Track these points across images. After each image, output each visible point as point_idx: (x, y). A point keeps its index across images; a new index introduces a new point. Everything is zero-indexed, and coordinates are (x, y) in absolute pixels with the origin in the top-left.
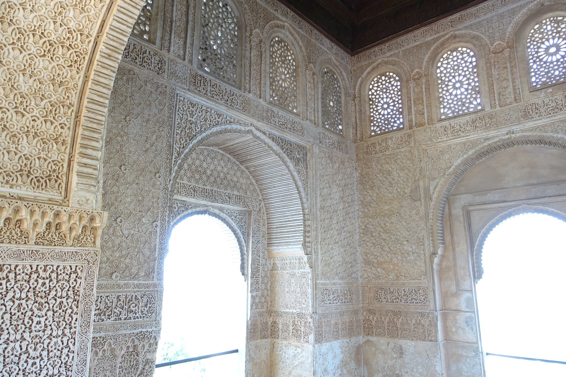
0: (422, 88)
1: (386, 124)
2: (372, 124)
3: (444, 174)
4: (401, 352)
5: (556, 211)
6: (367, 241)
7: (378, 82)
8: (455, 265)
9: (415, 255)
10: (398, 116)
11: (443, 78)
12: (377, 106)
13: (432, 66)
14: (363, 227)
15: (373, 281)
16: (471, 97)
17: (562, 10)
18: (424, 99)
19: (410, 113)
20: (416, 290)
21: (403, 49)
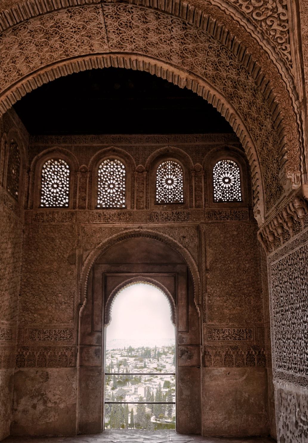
0: (86, 180)
1: (54, 200)
2: (42, 197)
3: (95, 247)
4: (47, 377)
5: (157, 282)
6: (28, 292)
7: (51, 164)
8: (92, 314)
9: (66, 305)
10: (64, 197)
11: (102, 178)
12: (48, 184)
13: (96, 166)
14: (25, 280)
15: (29, 324)
16: (119, 197)
17: (177, 159)
18: (87, 189)
19: (75, 196)
20: (65, 331)
21: (75, 145)
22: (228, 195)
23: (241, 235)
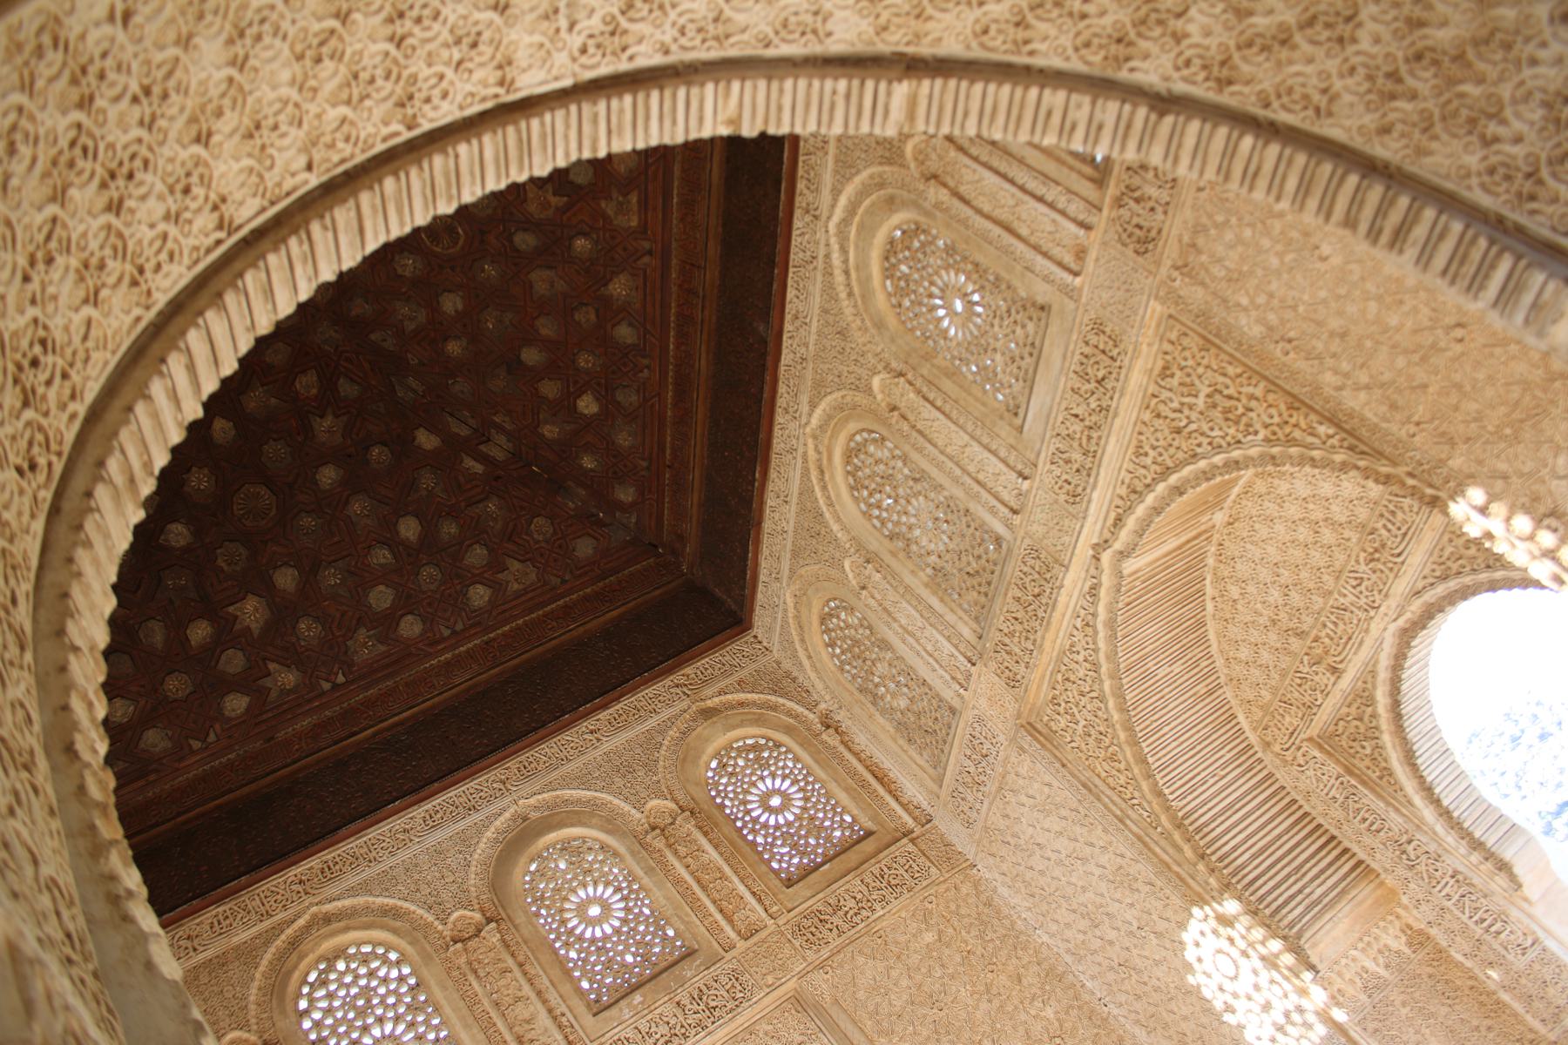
13: (283, 1012)
17: (572, 825)
22: (812, 841)
23: (951, 930)
